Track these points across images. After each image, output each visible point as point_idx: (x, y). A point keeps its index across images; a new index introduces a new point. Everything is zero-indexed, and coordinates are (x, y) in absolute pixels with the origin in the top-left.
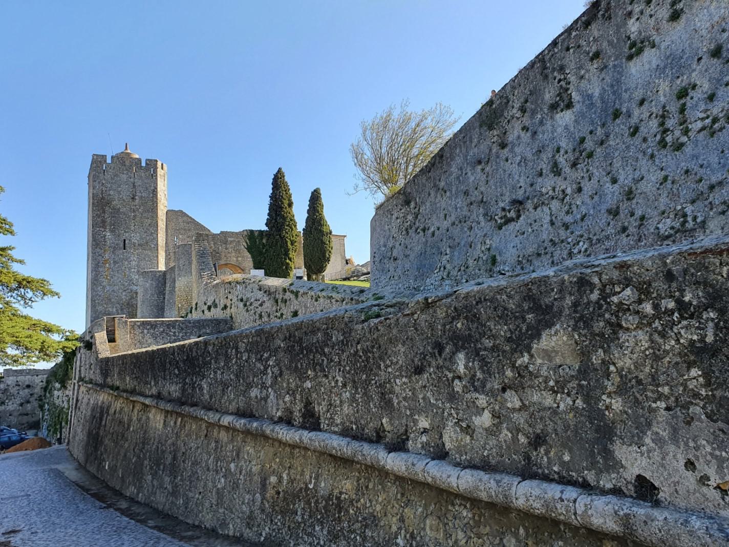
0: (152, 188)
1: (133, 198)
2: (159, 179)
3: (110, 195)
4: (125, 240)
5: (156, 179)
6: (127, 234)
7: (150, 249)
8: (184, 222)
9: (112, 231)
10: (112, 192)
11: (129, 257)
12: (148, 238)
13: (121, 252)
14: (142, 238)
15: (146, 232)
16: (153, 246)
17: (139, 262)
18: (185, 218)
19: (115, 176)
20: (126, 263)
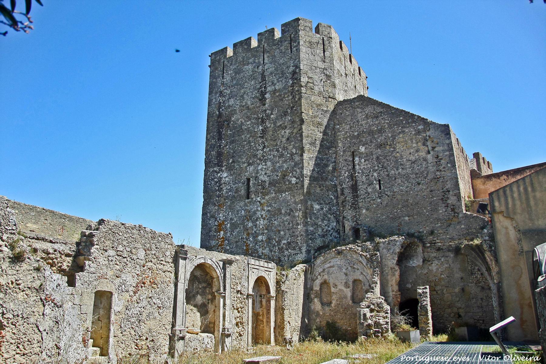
0: (291, 69)
1: (262, 100)
2: (303, 49)
3: (229, 106)
4: (249, 180)
5: (298, 50)
6: (252, 168)
7: (290, 189)
8: (367, 117)
9: (230, 169)
11: (255, 213)
12: (285, 166)
13: (242, 204)
14: (274, 170)
15: (282, 156)
16: (294, 180)
17: (270, 220)
18: (369, 109)
19: (236, 73)
20: (250, 224)
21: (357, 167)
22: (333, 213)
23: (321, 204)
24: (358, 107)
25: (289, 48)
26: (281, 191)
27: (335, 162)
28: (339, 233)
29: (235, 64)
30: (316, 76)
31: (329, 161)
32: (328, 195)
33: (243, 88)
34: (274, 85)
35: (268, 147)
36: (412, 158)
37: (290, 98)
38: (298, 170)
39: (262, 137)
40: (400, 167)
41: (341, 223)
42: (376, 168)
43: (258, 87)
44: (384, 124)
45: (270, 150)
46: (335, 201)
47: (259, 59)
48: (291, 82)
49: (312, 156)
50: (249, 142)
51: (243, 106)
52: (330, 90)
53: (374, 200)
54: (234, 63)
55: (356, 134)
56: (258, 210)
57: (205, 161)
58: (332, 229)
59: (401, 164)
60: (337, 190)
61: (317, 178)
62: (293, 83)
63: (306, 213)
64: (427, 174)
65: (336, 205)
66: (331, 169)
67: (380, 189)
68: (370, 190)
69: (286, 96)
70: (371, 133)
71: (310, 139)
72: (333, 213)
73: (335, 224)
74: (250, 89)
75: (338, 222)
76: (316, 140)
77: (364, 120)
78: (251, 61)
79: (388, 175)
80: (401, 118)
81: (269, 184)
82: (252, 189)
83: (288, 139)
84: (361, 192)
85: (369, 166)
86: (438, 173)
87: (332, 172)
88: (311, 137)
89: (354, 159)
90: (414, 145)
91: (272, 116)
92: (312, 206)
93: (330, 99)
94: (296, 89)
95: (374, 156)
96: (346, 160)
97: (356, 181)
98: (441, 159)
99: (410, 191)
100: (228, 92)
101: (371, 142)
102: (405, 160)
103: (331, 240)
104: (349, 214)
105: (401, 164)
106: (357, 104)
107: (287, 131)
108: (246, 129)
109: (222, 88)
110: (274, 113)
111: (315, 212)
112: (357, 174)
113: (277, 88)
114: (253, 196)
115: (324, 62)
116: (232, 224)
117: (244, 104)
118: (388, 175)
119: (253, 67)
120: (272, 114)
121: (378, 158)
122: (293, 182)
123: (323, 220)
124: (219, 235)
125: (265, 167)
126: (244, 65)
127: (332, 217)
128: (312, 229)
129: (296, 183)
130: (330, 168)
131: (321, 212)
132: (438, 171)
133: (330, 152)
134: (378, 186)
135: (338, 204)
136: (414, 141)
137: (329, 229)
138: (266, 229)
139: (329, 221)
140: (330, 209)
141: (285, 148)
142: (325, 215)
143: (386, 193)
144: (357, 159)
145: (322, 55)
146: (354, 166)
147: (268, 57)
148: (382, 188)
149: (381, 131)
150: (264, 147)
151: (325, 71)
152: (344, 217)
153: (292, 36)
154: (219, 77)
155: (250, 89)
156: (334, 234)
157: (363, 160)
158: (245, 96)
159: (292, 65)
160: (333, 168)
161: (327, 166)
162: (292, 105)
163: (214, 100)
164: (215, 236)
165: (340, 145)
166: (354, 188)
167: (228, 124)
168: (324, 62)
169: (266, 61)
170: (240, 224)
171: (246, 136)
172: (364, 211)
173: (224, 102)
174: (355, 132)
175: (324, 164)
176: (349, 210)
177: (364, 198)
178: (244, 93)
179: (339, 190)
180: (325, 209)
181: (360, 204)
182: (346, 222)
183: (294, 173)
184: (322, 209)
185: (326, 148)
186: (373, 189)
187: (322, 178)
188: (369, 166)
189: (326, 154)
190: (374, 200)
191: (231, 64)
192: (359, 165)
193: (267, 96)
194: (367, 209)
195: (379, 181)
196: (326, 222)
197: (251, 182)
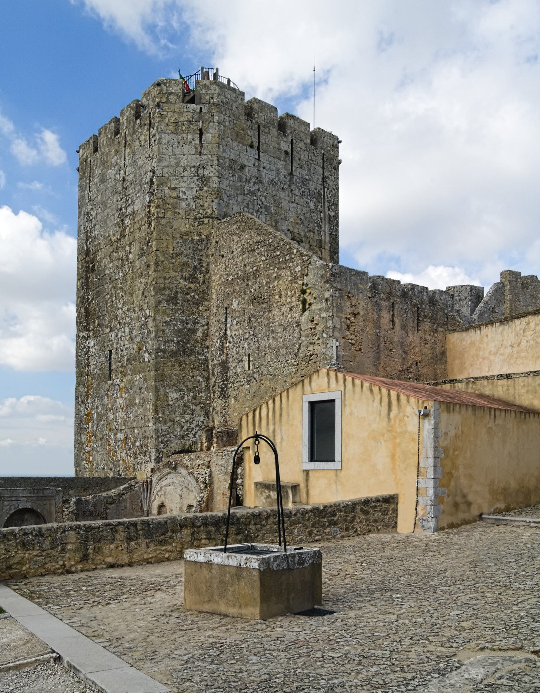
21: (228, 332)
22: (200, 403)
23: (180, 391)
24: (235, 234)
26: (135, 372)
27: (208, 324)
30: (183, 184)
31: (198, 323)
32: (193, 376)
36: (285, 322)
37: (147, 226)
38: (150, 342)
39: (122, 289)
40: (272, 335)
41: (211, 417)
42: (247, 335)
43: (119, 207)
44: (259, 262)
45: (129, 310)
46: (204, 384)
48: (148, 199)
49: (168, 319)
50: (111, 296)
52: (206, 205)
53: (242, 386)
55: (230, 278)
56: (118, 398)
57: (77, 322)
58: (197, 425)
59: (273, 332)
60: (208, 367)
61: (176, 352)
63: (156, 406)
64: (299, 349)
65: (205, 390)
66: (201, 335)
67: (249, 369)
68: (239, 370)
70: (245, 278)
71: (167, 292)
72: (200, 403)
73: (202, 418)
75: (207, 414)
76: (177, 292)
77: (240, 256)
79: (258, 347)
80: (278, 253)
81: (127, 360)
82: (114, 367)
83: (143, 293)
84: (231, 373)
85: (241, 332)
86: (311, 348)
87: (202, 340)
88: (169, 289)
89: (226, 320)
90: (289, 300)
92: (166, 395)
93: (206, 221)
95: (247, 317)
96: (218, 321)
97: (227, 355)
98: (317, 324)
99: (278, 375)
101: (245, 293)
102: (277, 324)
104: (218, 404)
105: (273, 332)
106: (235, 227)
107: (144, 280)
110: (132, 251)
111: (171, 403)
112: (228, 344)
114: (114, 377)
115: (200, 153)
116: (98, 414)
118: (258, 347)
120: (130, 252)
121: (250, 319)
122: (146, 360)
123: (182, 415)
124: (88, 428)
125: (123, 334)
127: (199, 407)
128: (164, 427)
129: (149, 361)
130: (199, 334)
131: (181, 403)
132: (311, 343)
133: (200, 308)
134: (247, 366)
135: (209, 389)
136: (289, 293)
137: (192, 426)
138: (124, 425)
139: (192, 414)
140: (195, 398)
141: (141, 309)
142: (185, 405)
143: (255, 376)
144: (229, 319)
145: (198, 142)
146: (226, 330)
148: (251, 368)
149: (256, 274)
151: (201, 171)
152: (214, 409)
157: (235, 322)
159: (150, 169)
160: (203, 333)
161: (194, 331)
163: (82, 227)
164: (85, 428)
165: (214, 297)
166: (224, 366)
168: (200, 153)
169: (127, 162)
170: (104, 415)
171: (108, 287)
172: (233, 401)
174: (230, 275)
175: (189, 330)
176: (219, 398)
177: (233, 382)
179: (210, 367)
180: (186, 398)
181: (230, 390)
182: (215, 416)
183: (147, 345)
184: (183, 398)
185: (194, 303)
186: (242, 368)
187: (184, 352)
188: (241, 332)
189: (193, 314)
190: (242, 386)
192: (230, 329)
193: (127, 221)
194: (236, 399)
195: (249, 354)
196: (187, 417)
197: (113, 356)
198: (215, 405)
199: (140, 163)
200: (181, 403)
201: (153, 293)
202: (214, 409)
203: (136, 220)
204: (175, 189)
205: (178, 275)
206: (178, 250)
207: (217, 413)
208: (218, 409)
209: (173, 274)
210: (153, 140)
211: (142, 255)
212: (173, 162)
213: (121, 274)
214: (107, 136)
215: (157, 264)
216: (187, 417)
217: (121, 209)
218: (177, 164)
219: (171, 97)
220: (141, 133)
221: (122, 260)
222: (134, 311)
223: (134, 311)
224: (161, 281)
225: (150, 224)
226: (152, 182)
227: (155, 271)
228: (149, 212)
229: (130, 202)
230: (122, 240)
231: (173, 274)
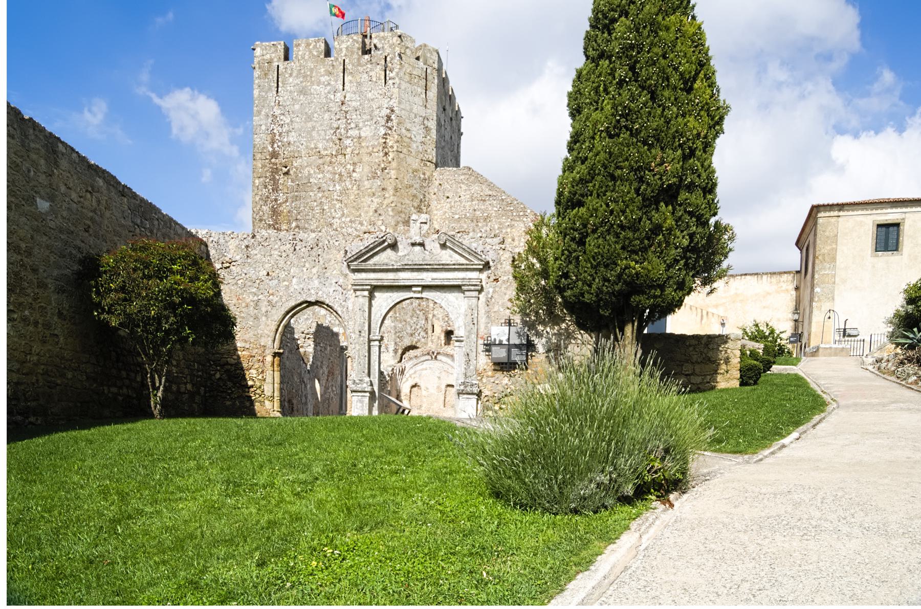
10: (292, 137)
25: (383, 77)
28: (427, 333)
29: (297, 77)
33: (311, 120)
34: (359, 129)
35: (348, 216)
37: (381, 154)
43: (335, 126)
45: (351, 221)
47: (336, 81)
48: (383, 132)
51: (312, 149)
54: (294, 74)
62: (386, 134)
69: (375, 150)
71: (403, 216)
74: (321, 125)
78: (323, 79)
83: (376, 211)
91: (354, 175)
94: (390, 144)
100: (288, 121)
103: (419, 340)
108: (316, 184)
109: (277, 112)
110: (357, 170)
113: (363, 134)
117: (313, 146)
119: (326, 91)
123: (412, 317)
126: (312, 83)
147: (351, 82)
150: (343, 215)
152: (434, 316)
153: (388, 59)
154: (270, 89)
155: (321, 125)
156: (423, 334)
158: (314, 134)
159: (386, 106)
162: (383, 166)
167: (289, 170)
173: (280, 135)
178: (314, 128)
191: (291, 75)
198: (435, 312)
199: (370, 95)
200: (410, 307)
201: (391, 213)
202: (434, 316)
203: (363, 144)
204: (408, 130)
205: (410, 203)
206: (411, 182)
207: (438, 319)
208: (440, 316)
209: (408, 202)
210: (390, 82)
211: (374, 178)
212: (408, 108)
213: (338, 187)
214: (310, 52)
215: (396, 190)
216: (415, 319)
217: (338, 128)
218: (411, 110)
219: (408, 50)
220: (371, 70)
221: (340, 175)
222: (361, 224)
223: (361, 224)
224: (399, 205)
225: (386, 154)
226: (389, 119)
227: (394, 195)
228: (385, 143)
229: (353, 125)
230: (340, 157)
231: (408, 202)
